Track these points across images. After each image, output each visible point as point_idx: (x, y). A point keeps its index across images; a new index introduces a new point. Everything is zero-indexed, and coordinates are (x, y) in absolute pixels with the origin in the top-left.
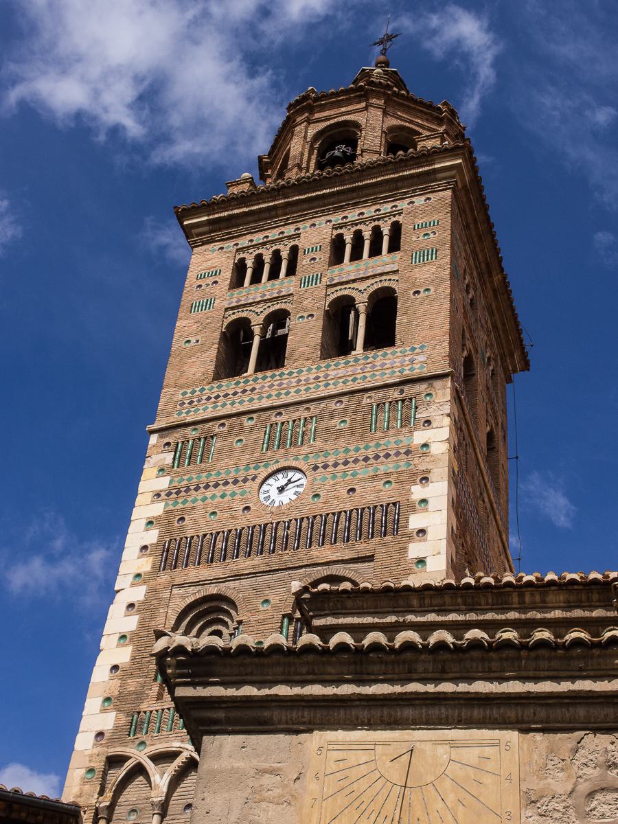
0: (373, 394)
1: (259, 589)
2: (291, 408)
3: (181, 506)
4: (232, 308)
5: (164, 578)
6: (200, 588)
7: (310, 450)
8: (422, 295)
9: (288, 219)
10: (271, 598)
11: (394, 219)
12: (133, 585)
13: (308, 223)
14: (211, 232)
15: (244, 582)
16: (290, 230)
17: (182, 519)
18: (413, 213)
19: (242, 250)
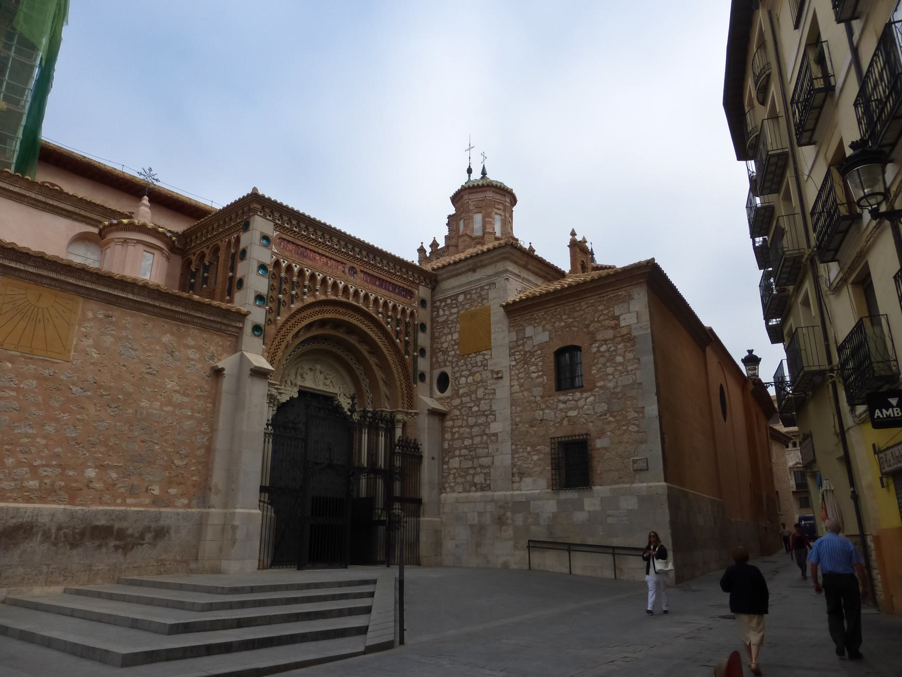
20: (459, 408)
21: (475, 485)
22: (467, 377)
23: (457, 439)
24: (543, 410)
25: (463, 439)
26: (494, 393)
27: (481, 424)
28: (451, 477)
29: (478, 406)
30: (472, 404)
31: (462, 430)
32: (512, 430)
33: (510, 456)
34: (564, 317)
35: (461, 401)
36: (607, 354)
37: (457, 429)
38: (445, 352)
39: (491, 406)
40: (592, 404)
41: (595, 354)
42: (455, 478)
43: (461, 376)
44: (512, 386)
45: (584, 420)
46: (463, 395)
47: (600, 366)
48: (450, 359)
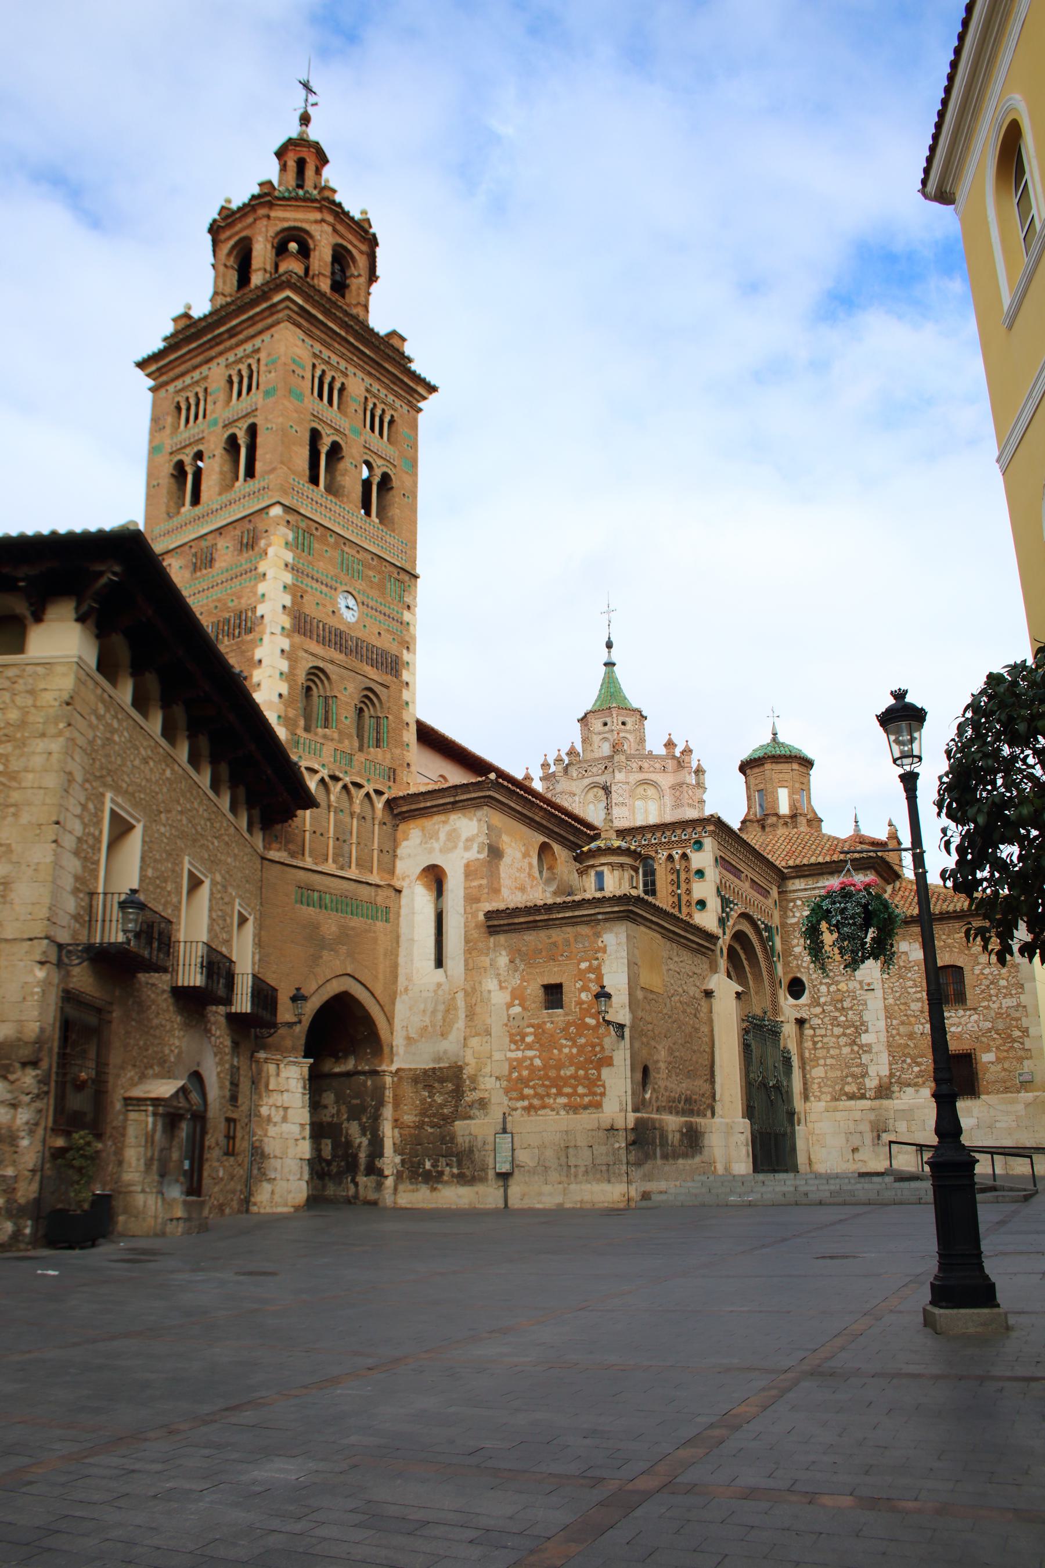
0: (387, 564)
1: (342, 678)
2: (351, 544)
3: (299, 584)
4: (314, 416)
5: (298, 639)
6: (314, 659)
7: (361, 587)
8: (406, 499)
9: (344, 354)
10: (348, 688)
11: (393, 413)
12: (282, 635)
13: (351, 370)
14: (296, 313)
15: (336, 669)
16: (343, 365)
17: (302, 597)
18: (402, 416)
19: (315, 355)
20: (821, 1016)
21: (846, 1094)
22: (828, 985)
23: (821, 1048)
24: (922, 1024)
25: (828, 1049)
26: (866, 1004)
27: (850, 1034)
28: (815, 1086)
29: (846, 1016)
30: (837, 1014)
31: (825, 1040)
32: (888, 1042)
33: (887, 1067)
34: (944, 937)
35: (824, 1010)
36: (990, 977)
37: (820, 1038)
38: (796, 958)
39: (861, 1017)
40: (976, 1022)
41: (978, 975)
42: (820, 1087)
43: (821, 983)
44: (885, 999)
45: (968, 1036)
46: (825, 1004)
47: (983, 987)
48: (805, 965)
